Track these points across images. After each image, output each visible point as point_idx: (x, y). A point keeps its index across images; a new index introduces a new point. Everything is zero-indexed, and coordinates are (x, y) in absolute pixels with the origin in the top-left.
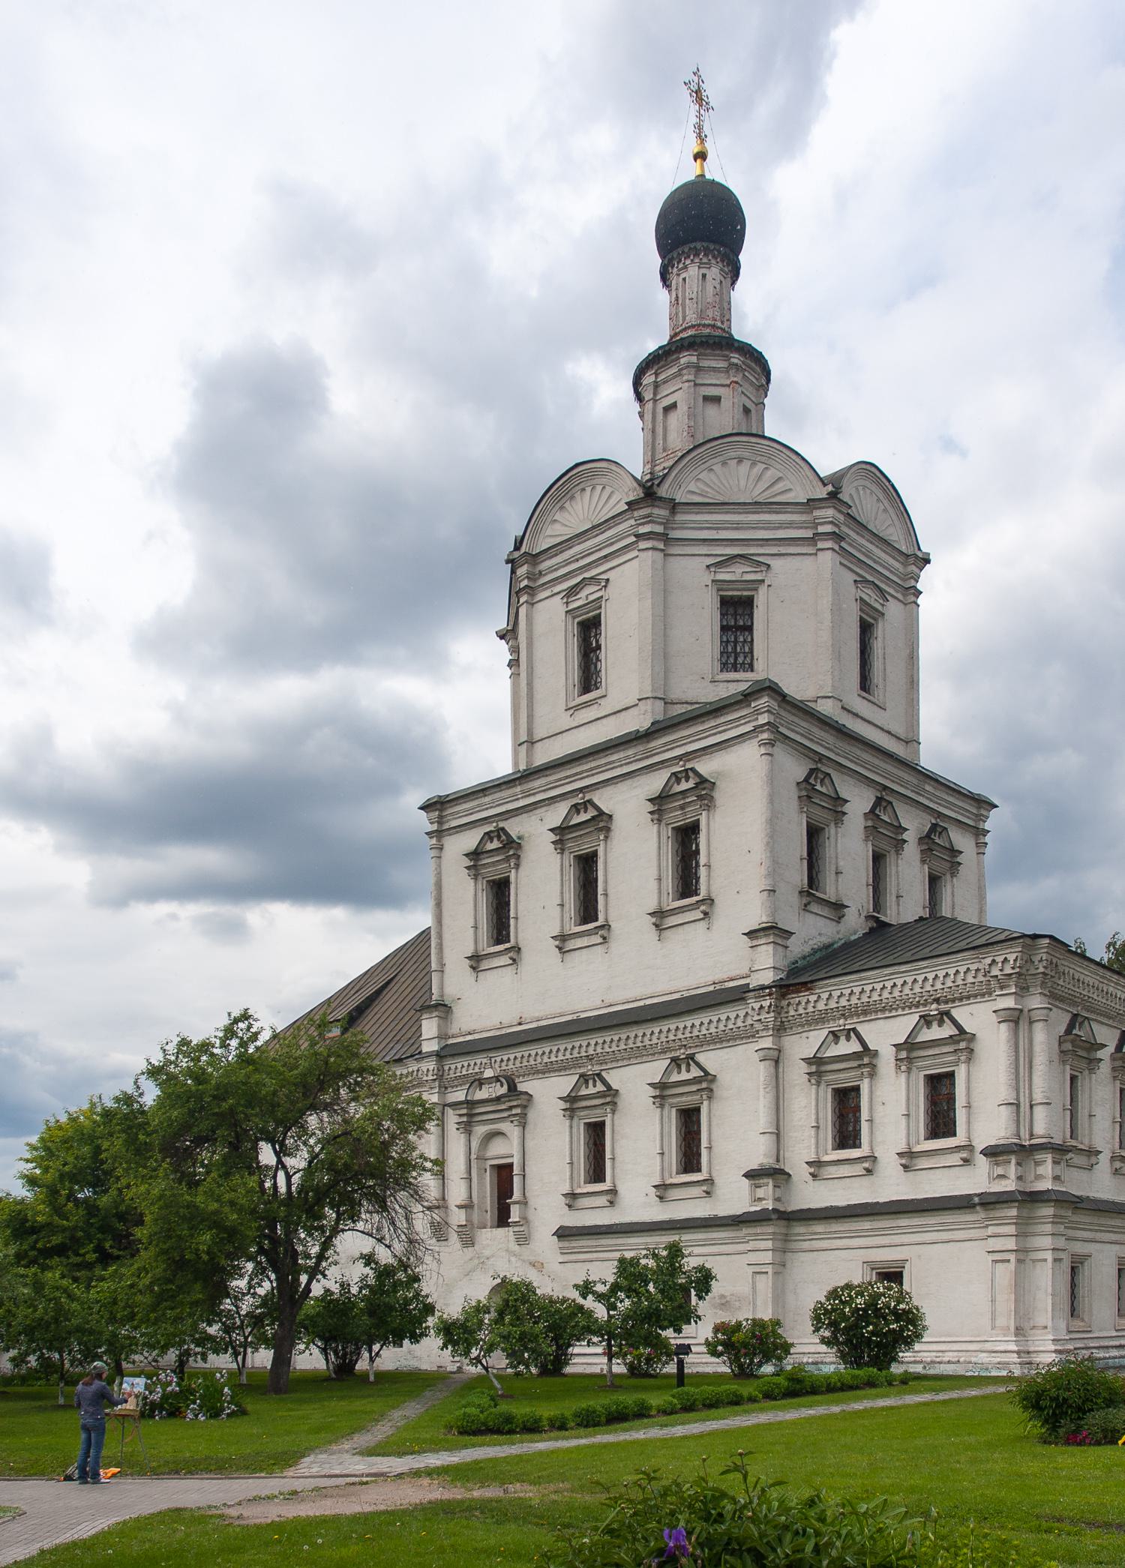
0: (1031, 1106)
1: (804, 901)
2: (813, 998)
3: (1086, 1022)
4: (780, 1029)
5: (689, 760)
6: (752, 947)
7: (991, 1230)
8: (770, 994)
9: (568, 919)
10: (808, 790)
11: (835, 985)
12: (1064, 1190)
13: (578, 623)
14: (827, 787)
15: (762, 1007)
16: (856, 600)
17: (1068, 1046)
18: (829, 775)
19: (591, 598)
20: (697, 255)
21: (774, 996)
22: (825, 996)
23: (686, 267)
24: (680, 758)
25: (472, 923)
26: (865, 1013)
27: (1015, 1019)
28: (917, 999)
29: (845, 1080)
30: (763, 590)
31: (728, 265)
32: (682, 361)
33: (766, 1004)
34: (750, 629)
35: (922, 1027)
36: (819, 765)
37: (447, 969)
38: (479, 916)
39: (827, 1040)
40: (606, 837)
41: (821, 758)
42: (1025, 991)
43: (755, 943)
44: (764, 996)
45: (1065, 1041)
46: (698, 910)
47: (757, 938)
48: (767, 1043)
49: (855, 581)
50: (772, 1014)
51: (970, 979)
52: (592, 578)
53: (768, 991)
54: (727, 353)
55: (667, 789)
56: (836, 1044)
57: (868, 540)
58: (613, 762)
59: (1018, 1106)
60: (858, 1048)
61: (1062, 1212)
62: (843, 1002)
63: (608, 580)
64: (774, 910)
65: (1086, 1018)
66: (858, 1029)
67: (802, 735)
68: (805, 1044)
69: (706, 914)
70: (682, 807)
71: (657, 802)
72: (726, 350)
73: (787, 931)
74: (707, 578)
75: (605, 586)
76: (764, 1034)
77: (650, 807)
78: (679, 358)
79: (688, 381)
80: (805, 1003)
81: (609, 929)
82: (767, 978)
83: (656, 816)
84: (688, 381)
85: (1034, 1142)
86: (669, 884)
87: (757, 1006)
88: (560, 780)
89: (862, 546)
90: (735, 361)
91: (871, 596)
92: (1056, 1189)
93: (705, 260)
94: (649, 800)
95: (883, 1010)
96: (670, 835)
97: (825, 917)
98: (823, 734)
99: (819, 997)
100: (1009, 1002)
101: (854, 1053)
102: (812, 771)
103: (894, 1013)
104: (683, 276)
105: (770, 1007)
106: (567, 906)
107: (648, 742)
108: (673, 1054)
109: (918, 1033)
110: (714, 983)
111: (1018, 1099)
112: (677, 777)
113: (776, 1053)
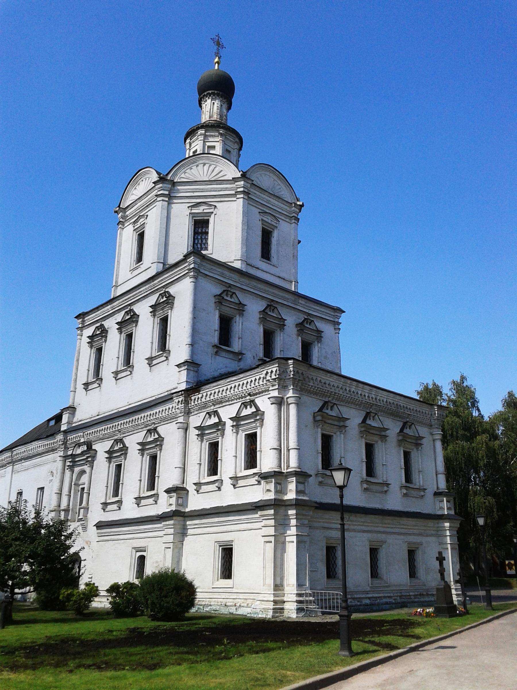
0: (288, 450)
1: (215, 350)
2: (200, 396)
3: (335, 406)
4: (188, 413)
5: (167, 288)
6: (179, 372)
7: (263, 524)
8: (182, 395)
9: (120, 364)
10: (220, 300)
11: (208, 389)
12: (307, 499)
13: (138, 235)
14: (234, 299)
15: (179, 402)
16: (260, 220)
17: (319, 418)
18: (235, 293)
19: (142, 223)
20: (210, 96)
21: (183, 396)
22: (205, 394)
23: (206, 101)
24: (163, 287)
25: (87, 368)
26: (221, 402)
27: (279, 402)
28: (241, 394)
29: (212, 437)
30: (213, 216)
31: (225, 99)
32: (199, 133)
33: (180, 399)
34: (207, 233)
35: (243, 409)
36: (229, 289)
37: (77, 390)
38: (91, 365)
39: (206, 417)
40: (136, 325)
41: (230, 286)
42: (286, 388)
43: (180, 369)
44: (179, 396)
45: (317, 416)
46: (163, 356)
47: (181, 367)
48: (181, 420)
49: (259, 212)
50: (183, 405)
51: (261, 383)
52: (143, 215)
53: (180, 393)
54: (218, 129)
55: (158, 301)
56: (210, 419)
57: (267, 196)
58: (141, 291)
59: (281, 450)
60: (217, 420)
61: (304, 512)
62: (212, 397)
63: (147, 215)
64: (193, 353)
65: (335, 404)
66: (219, 411)
67: (218, 275)
68: (196, 420)
69: (167, 357)
70: (162, 309)
71: (153, 307)
72: (218, 128)
73: (197, 364)
74: (188, 211)
75: (146, 218)
76: (180, 415)
77: (151, 310)
78: (197, 133)
79: (200, 140)
80: (197, 399)
81: (133, 368)
82: (183, 386)
83: (153, 314)
84: (200, 140)
85: (288, 470)
86: (156, 345)
87: (177, 401)
88: (123, 301)
89: (264, 198)
90: (221, 132)
91: (268, 219)
92: (300, 498)
93: (214, 97)
94: (150, 307)
95: (228, 401)
96: (159, 322)
97: (231, 359)
98: (231, 275)
99: (203, 395)
100: (275, 393)
101: (215, 423)
102: (224, 291)
103: (233, 402)
104: (205, 104)
105: (182, 401)
106: (120, 359)
107: (153, 282)
108: (148, 428)
109: (241, 412)
110: (168, 391)
111: (280, 446)
112: (162, 295)
113: (185, 425)
